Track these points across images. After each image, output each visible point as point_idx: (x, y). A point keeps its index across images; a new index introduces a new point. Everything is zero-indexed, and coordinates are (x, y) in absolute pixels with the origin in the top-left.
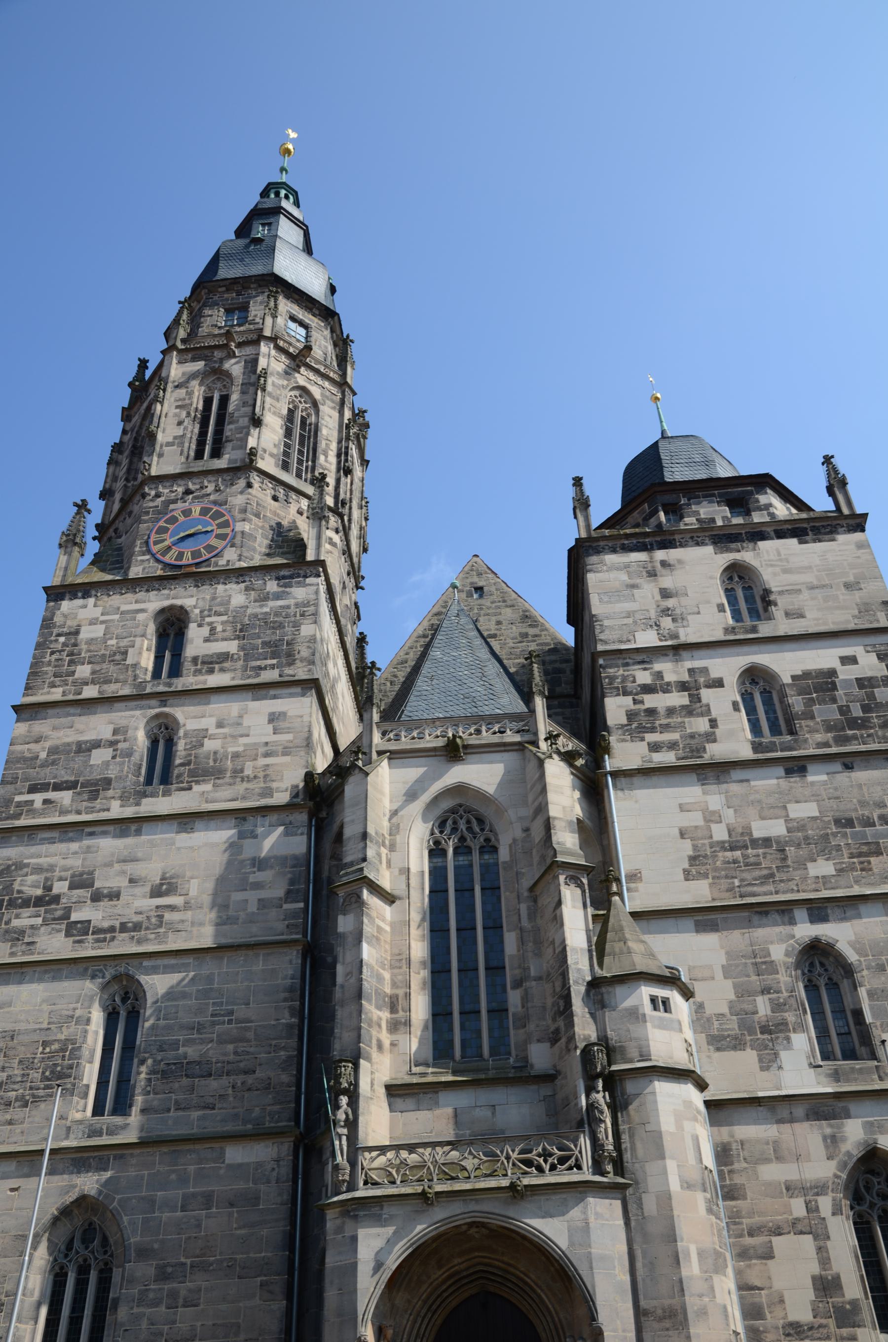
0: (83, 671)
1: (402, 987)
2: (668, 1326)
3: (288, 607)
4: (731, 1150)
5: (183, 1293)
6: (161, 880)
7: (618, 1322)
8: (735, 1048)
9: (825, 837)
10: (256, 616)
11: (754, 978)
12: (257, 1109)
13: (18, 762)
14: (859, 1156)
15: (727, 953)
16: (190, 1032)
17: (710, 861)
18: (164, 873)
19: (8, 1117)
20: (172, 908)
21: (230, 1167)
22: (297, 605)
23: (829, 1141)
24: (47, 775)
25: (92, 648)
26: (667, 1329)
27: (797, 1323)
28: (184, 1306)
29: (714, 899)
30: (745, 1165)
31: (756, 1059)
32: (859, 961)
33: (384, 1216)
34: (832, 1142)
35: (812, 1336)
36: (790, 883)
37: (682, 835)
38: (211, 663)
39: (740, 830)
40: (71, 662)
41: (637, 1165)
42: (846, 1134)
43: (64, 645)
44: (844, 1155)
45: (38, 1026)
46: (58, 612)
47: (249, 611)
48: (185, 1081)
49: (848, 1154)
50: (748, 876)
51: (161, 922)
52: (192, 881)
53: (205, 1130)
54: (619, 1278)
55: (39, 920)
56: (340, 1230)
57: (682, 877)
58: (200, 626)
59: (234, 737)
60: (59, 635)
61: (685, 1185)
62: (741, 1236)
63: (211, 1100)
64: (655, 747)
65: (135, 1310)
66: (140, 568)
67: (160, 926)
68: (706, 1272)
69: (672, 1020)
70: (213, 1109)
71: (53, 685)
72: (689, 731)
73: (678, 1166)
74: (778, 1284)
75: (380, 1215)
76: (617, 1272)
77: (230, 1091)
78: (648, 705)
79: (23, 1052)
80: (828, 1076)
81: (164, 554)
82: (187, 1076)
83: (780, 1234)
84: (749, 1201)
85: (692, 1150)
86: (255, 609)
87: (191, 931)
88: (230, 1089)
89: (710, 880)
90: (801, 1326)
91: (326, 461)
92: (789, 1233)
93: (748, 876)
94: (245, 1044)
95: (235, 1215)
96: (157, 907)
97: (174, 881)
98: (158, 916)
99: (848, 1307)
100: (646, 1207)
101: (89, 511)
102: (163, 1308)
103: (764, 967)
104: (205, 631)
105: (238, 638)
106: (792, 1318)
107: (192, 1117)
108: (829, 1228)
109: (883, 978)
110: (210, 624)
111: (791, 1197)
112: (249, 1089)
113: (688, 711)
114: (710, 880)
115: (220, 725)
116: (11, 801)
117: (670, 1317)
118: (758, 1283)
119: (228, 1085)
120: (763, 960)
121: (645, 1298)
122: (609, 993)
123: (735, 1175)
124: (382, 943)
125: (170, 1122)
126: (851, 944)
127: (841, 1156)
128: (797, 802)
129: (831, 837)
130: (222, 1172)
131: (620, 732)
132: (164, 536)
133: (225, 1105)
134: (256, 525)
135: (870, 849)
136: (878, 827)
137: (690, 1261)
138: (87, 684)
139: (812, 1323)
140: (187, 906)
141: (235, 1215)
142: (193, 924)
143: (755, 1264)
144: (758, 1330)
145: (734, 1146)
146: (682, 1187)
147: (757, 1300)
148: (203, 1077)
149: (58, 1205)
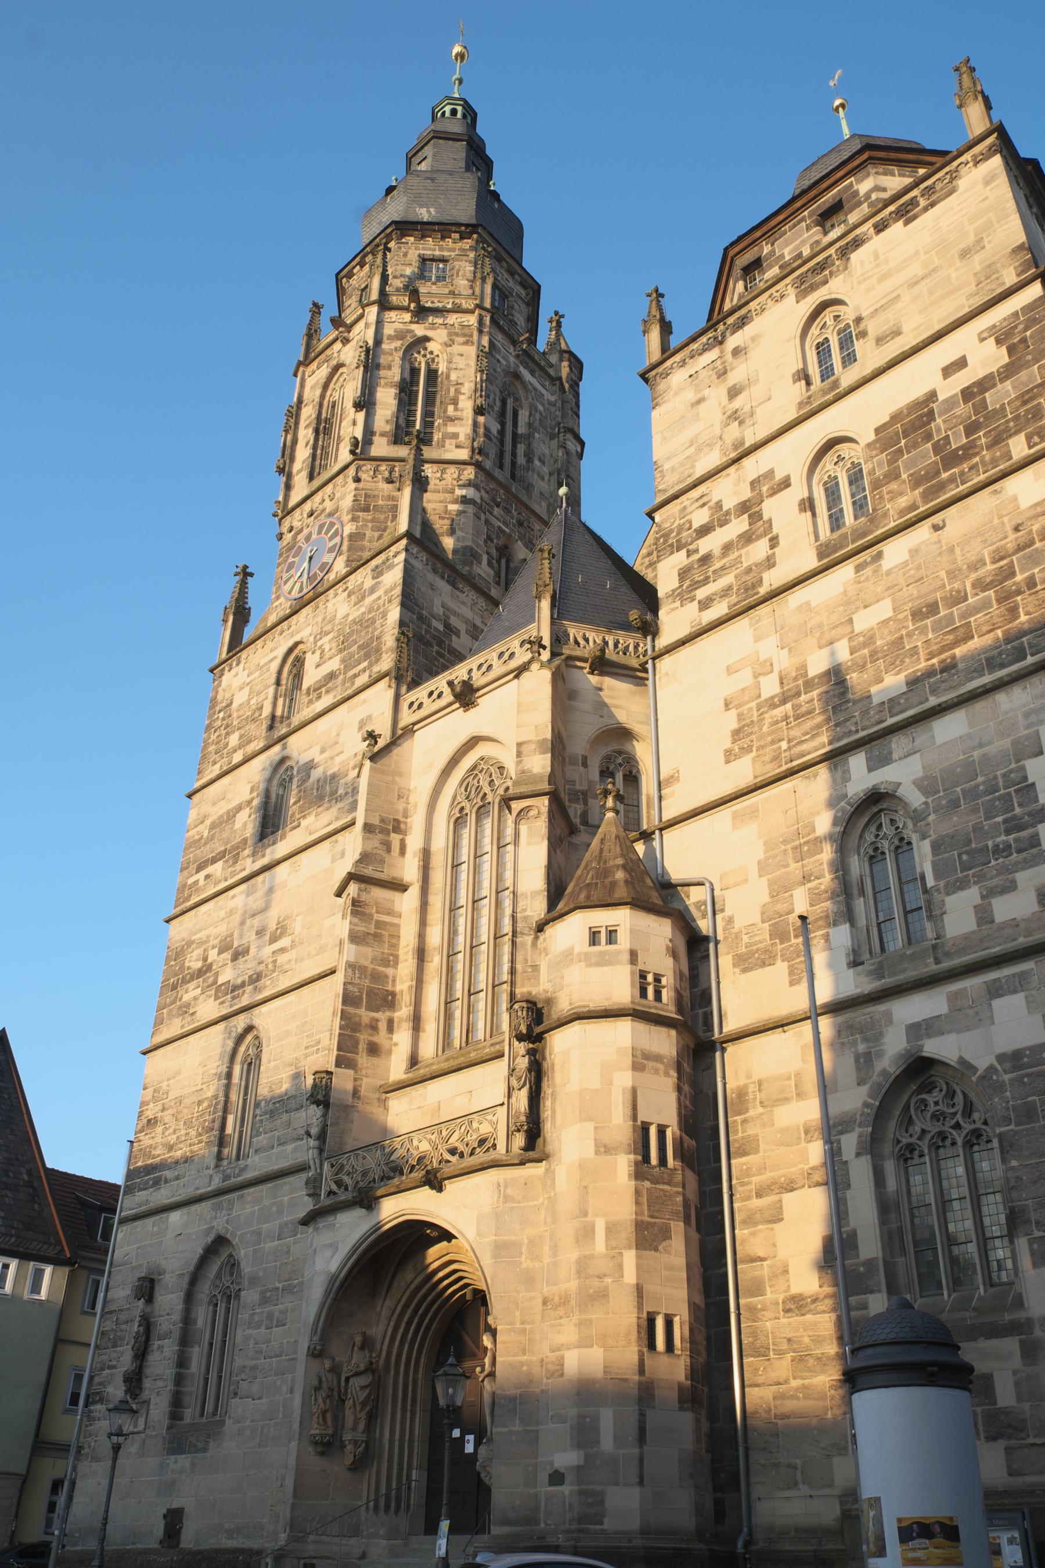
0: (234, 740)
2: (562, 1314)
3: (379, 598)
4: (747, 1094)
5: (277, 1314)
7: (518, 1314)
8: (764, 964)
9: (898, 643)
10: (354, 622)
11: (793, 866)
13: (191, 847)
14: (898, 1073)
15: (765, 844)
17: (756, 729)
19: (176, 1173)
20: (283, 950)
22: (386, 593)
23: (862, 1060)
24: (207, 852)
25: (240, 713)
26: (561, 1318)
27: (801, 1295)
28: (277, 1326)
29: (756, 777)
30: (761, 1110)
31: (786, 971)
32: (926, 803)
34: (865, 1062)
35: (815, 1309)
36: (848, 723)
37: (727, 705)
38: (320, 688)
39: (794, 674)
40: (228, 734)
41: (555, 1135)
42: (884, 1047)
43: (223, 719)
44: (879, 1075)
45: (195, 1089)
46: (220, 689)
47: (351, 618)
49: (884, 1072)
50: (796, 733)
51: (275, 966)
54: (524, 1265)
55: (199, 990)
58: (313, 653)
59: (332, 758)
60: (220, 711)
61: (603, 1150)
62: (748, 1198)
64: (705, 604)
65: (247, 1332)
66: (275, 614)
67: (274, 971)
68: (615, 1248)
71: (215, 763)
72: (745, 565)
73: (595, 1128)
74: (782, 1253)
75: (334, 1225)
76: (523, 1259)
78: (702, 552)
79: (186, 1114)
80: (870, 973)
81: (290, 593)
83: (792, 1190)
84: (761, 1154)
85: (620, 1108)
86: (355, 614)
89: (754, 754)
90: (803, 1299)
91: (456, 409)
92: (803, 1186)
93: (796, 733)
96: (273, 953)
99: (862, 1269)
101: (251, 575)
102: (263, 1330)
103: (806, 848)
104: (316, 657)
105: (340, 651)
106: (795, 1290)
108: (851, 1173)
109: (955, 819)
110: (320, 648)
111: (810, 1141)
113: (747, 538)
115: (323, 751)
116: (185, 885)
118: (761, 1254)
120: (806, 839)
123: (749, 1125)
124: (386, 939)
126: (918, 784)
127: (874, 1077)
128: (866, 607)
129: (905, 640)
131: (670, 599)
132: (292, 572)
134: (364, 520)
135: (957, 636)
136: (970, 600)
137: (593, 1238)
138: (235, 751)
139: (818, 1293)
140: (293, 945)
143: (760, 1231)
144: (755, 1309)
145: (751, 1089)
146: (597, 1153)
147: (757, 1273)
149: (203, 1245)
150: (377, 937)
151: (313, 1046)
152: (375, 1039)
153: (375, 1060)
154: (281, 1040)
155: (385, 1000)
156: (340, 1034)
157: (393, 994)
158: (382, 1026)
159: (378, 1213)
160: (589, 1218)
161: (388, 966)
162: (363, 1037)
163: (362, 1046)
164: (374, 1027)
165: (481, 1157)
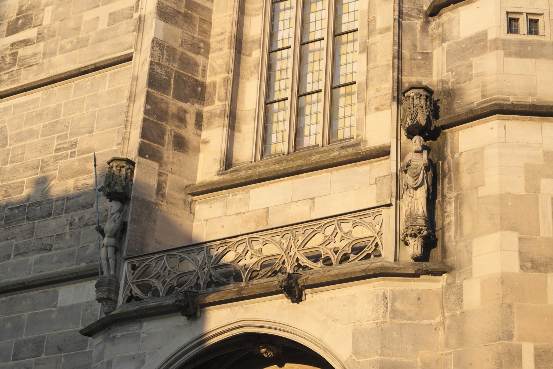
1: (221, 73)
6: (18, 14)
12: (92, 245)
16: (34, 171)
18: (21, 7)
20: (26, 43)
21: (62, 310)
33: (142, 336)
41: (461, 245)
48: (26, 224)
51: (15, 60)
52: (47, 9)
53: (41, 274)
61: (529, 265)
63: (48, 241)
67: (13, 65)
69: (543, 44)
70: (50, 250)
73: (520, 239)
75: (139, 335)
77: (67, 229)
82: (28, 219)
87: (43, 63)
88: (68, 226)
94: (85, 176)
95: (63, 360)
96: (12, 45)
97: (30, 12)
98: (13, 54)
100: (466, 298)
107: (30, 261)
112: (86, 225)
119: (66, 222)
122: (451, 20)
124: (197, 23)
125: (9, 269)
130: (53, 316)
133: (61, 245)
140: (40, 37)
141: (63, 360)
142: (44, 55)
146: (522, 267)
148: (43, 217)
150: (187, 18)
151: (66, 149)
152: (183, 132)
153: (181, 156)
154: (22, 140)
155: (194, 91)
156: (145, 120)
157: (203, 85)
158: (191, 119)
159: (203, 325)
160: (515, 342)
161: (198, 53)
162: (170, 128)
163: (168, 138)
164: (181, 118)
165: (356, 264)
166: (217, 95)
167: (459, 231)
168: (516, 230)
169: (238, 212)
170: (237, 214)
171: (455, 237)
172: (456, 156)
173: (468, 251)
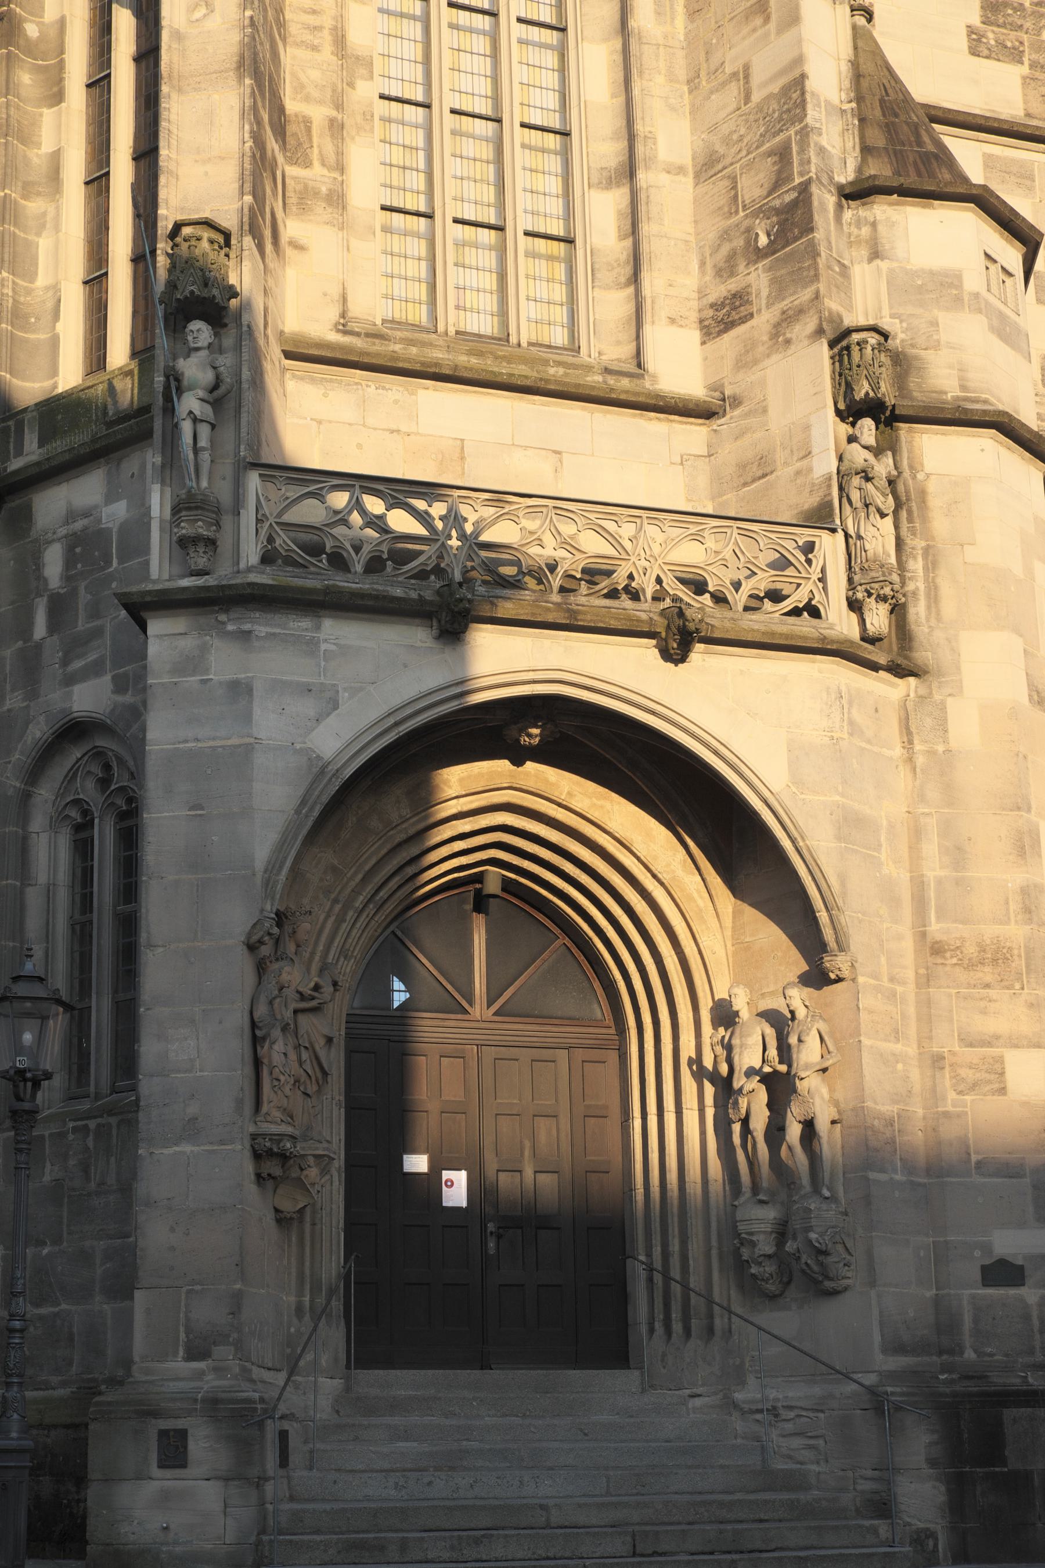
1: (321, 102)
2: (988, 978)
7: (883, 960)
26: (987, 986)
33: (324, 647)
56: (192, 664)
57: (964, 43)
114: (1025, 69)
117: (995, 961)
121: (939, 919)
160: (1033, 817)
165: (771, 619)
166: (316, 150)
167: (933, 610)
168: (1021, 636)
169: (395, 427)
170: (392, 432)
171: (928, 620)
172: (920, 476)
173: (952, 649)
